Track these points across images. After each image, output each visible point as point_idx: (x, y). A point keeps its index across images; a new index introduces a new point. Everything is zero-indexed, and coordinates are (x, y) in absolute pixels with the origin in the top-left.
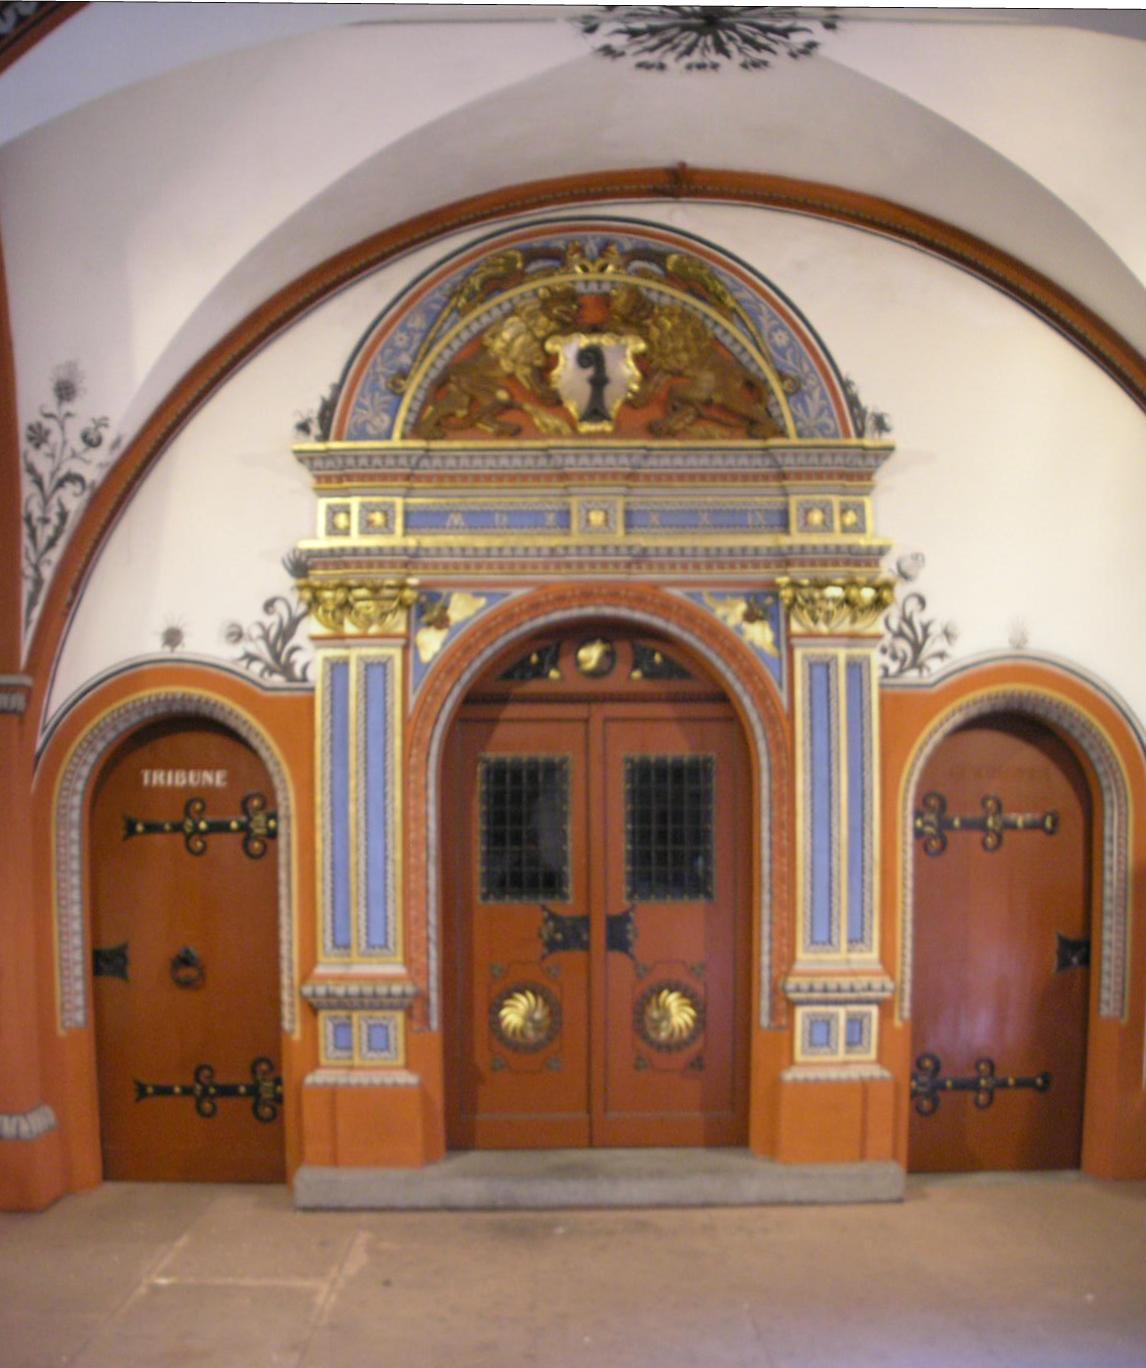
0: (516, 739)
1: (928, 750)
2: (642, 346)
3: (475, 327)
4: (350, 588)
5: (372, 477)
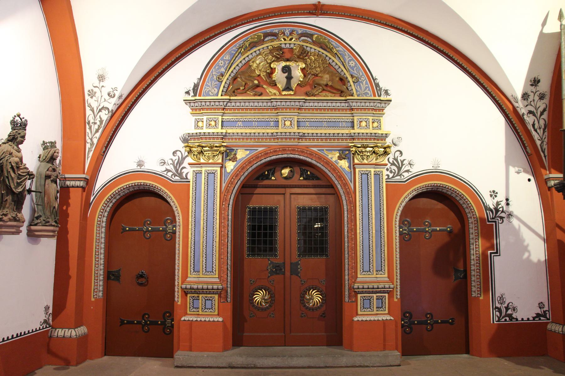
0: (261, 200)
1: (404, 204)
2: (304, 66)
3: (247, 59)
4: (203, 147)
5: (211, 109)
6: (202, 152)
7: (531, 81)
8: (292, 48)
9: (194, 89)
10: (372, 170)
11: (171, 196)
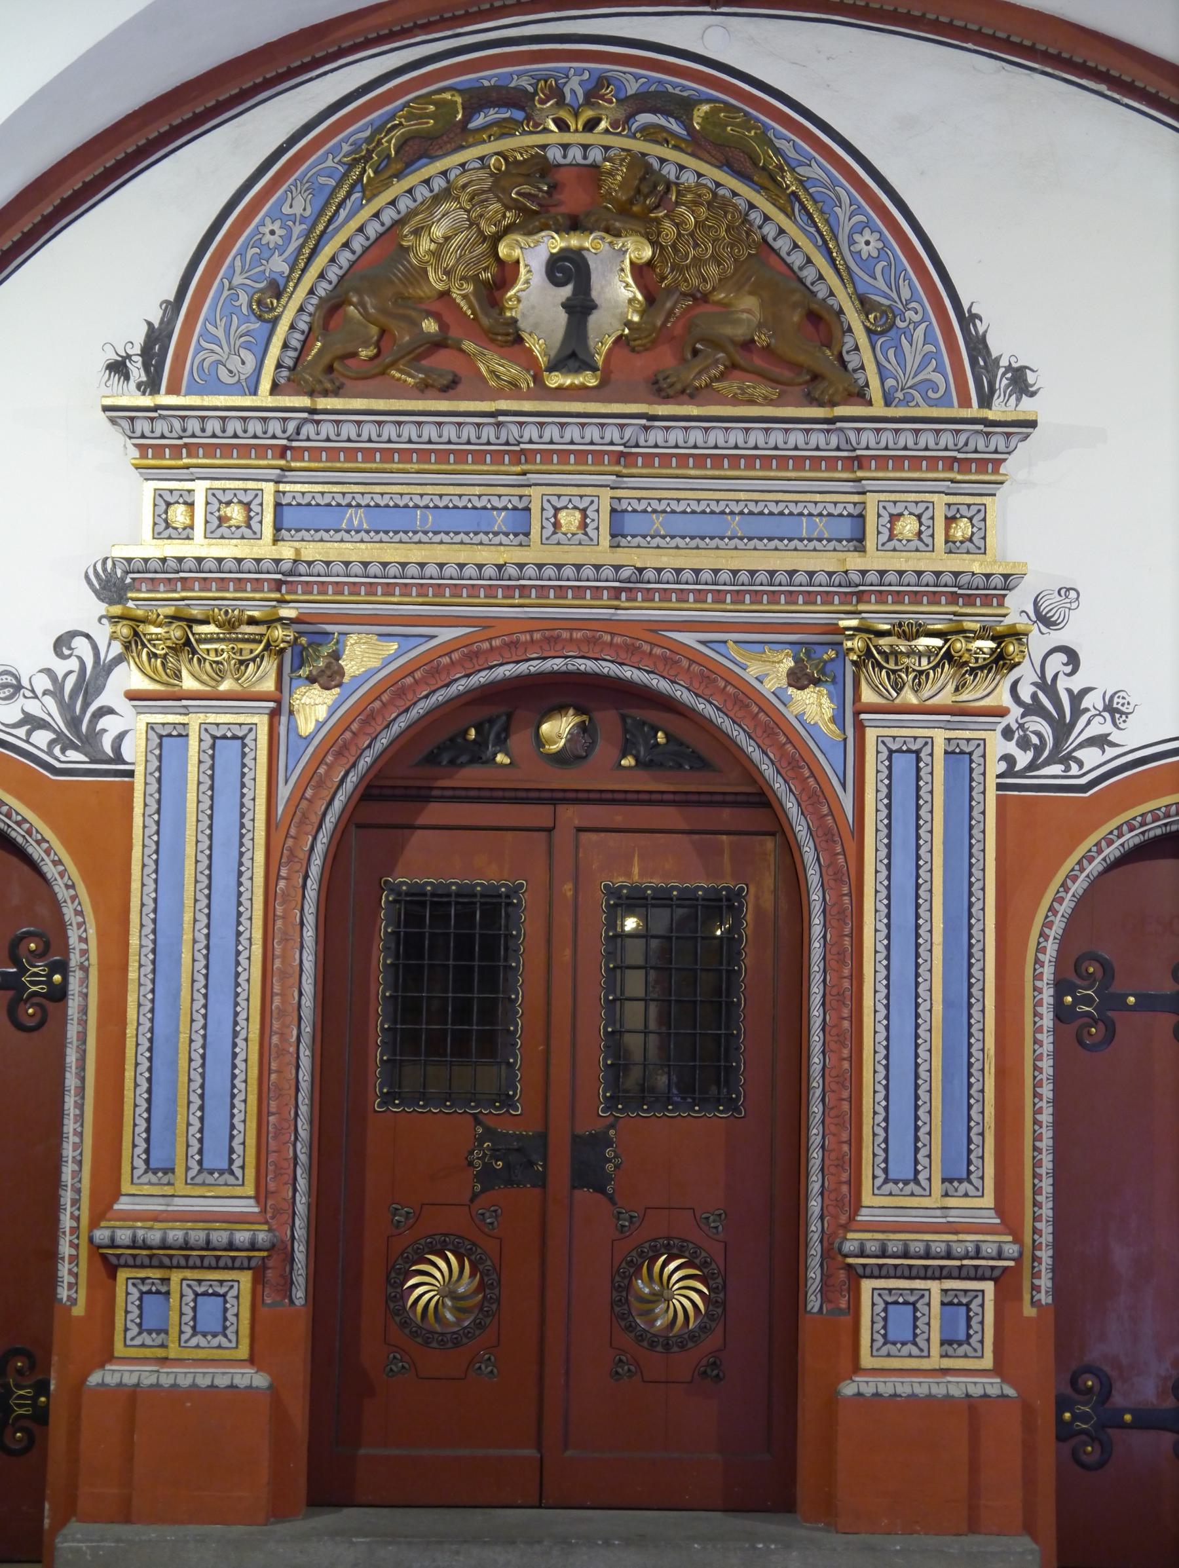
1: (1078, 886)
2: (647, 253)
3: (389, 216)
4: (192, 621)
5: (227, 451)
6: (188, 643)
8: (595, 166)
9: (146, 352)
11: (48, 834)
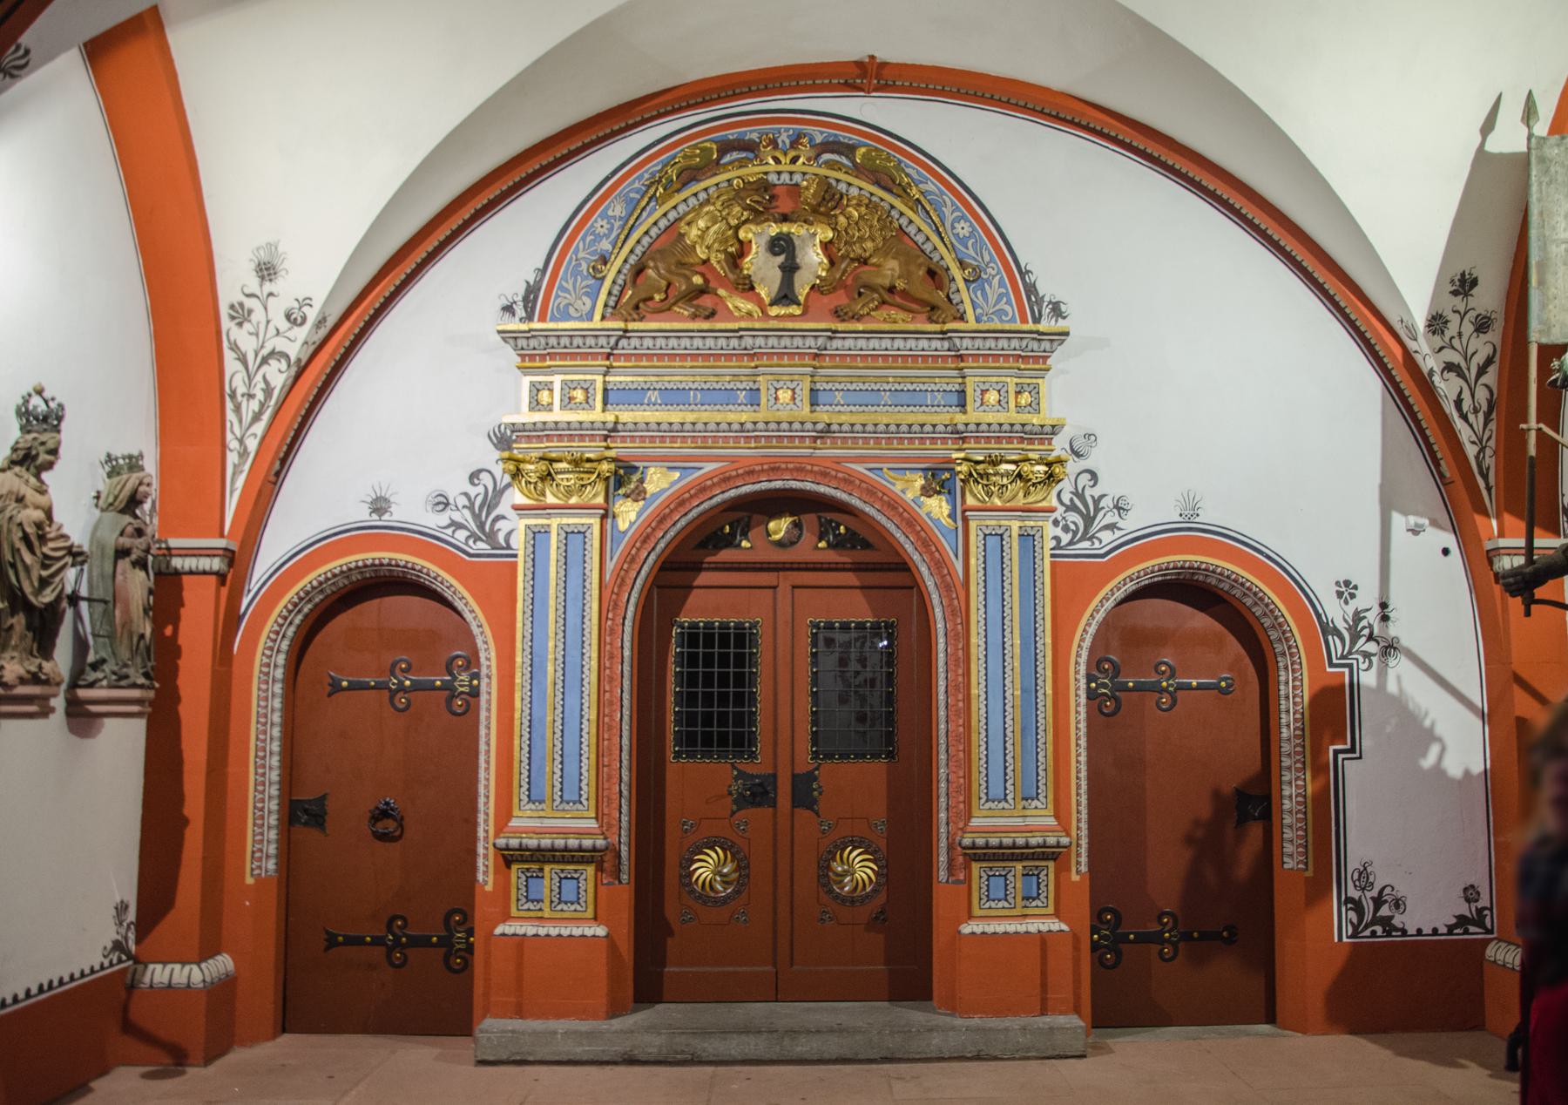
0: (706, 605)
1: (1099, 617)
2: (830, 235)
3: (672, 215)
4: (552, 461)
5: (573, 356)
6: (549, 474)
7: (1452, 281)
8: (797, 185)
9: (526, 299)
10: (1015, 525)
11: (466, 594)
